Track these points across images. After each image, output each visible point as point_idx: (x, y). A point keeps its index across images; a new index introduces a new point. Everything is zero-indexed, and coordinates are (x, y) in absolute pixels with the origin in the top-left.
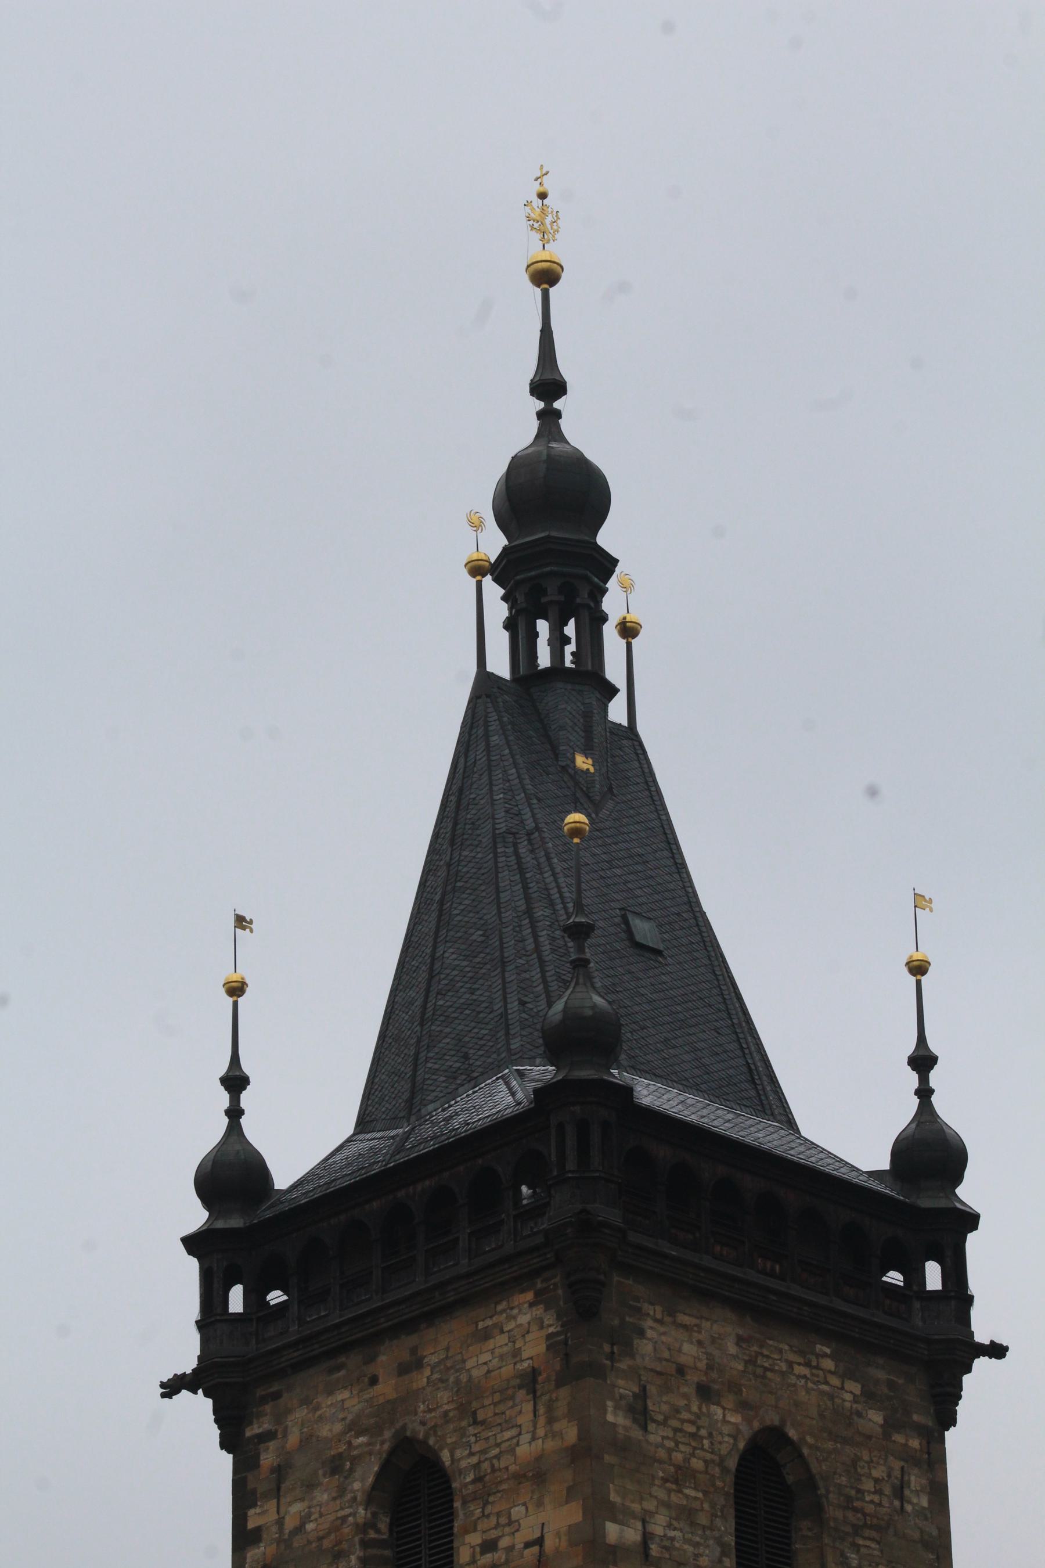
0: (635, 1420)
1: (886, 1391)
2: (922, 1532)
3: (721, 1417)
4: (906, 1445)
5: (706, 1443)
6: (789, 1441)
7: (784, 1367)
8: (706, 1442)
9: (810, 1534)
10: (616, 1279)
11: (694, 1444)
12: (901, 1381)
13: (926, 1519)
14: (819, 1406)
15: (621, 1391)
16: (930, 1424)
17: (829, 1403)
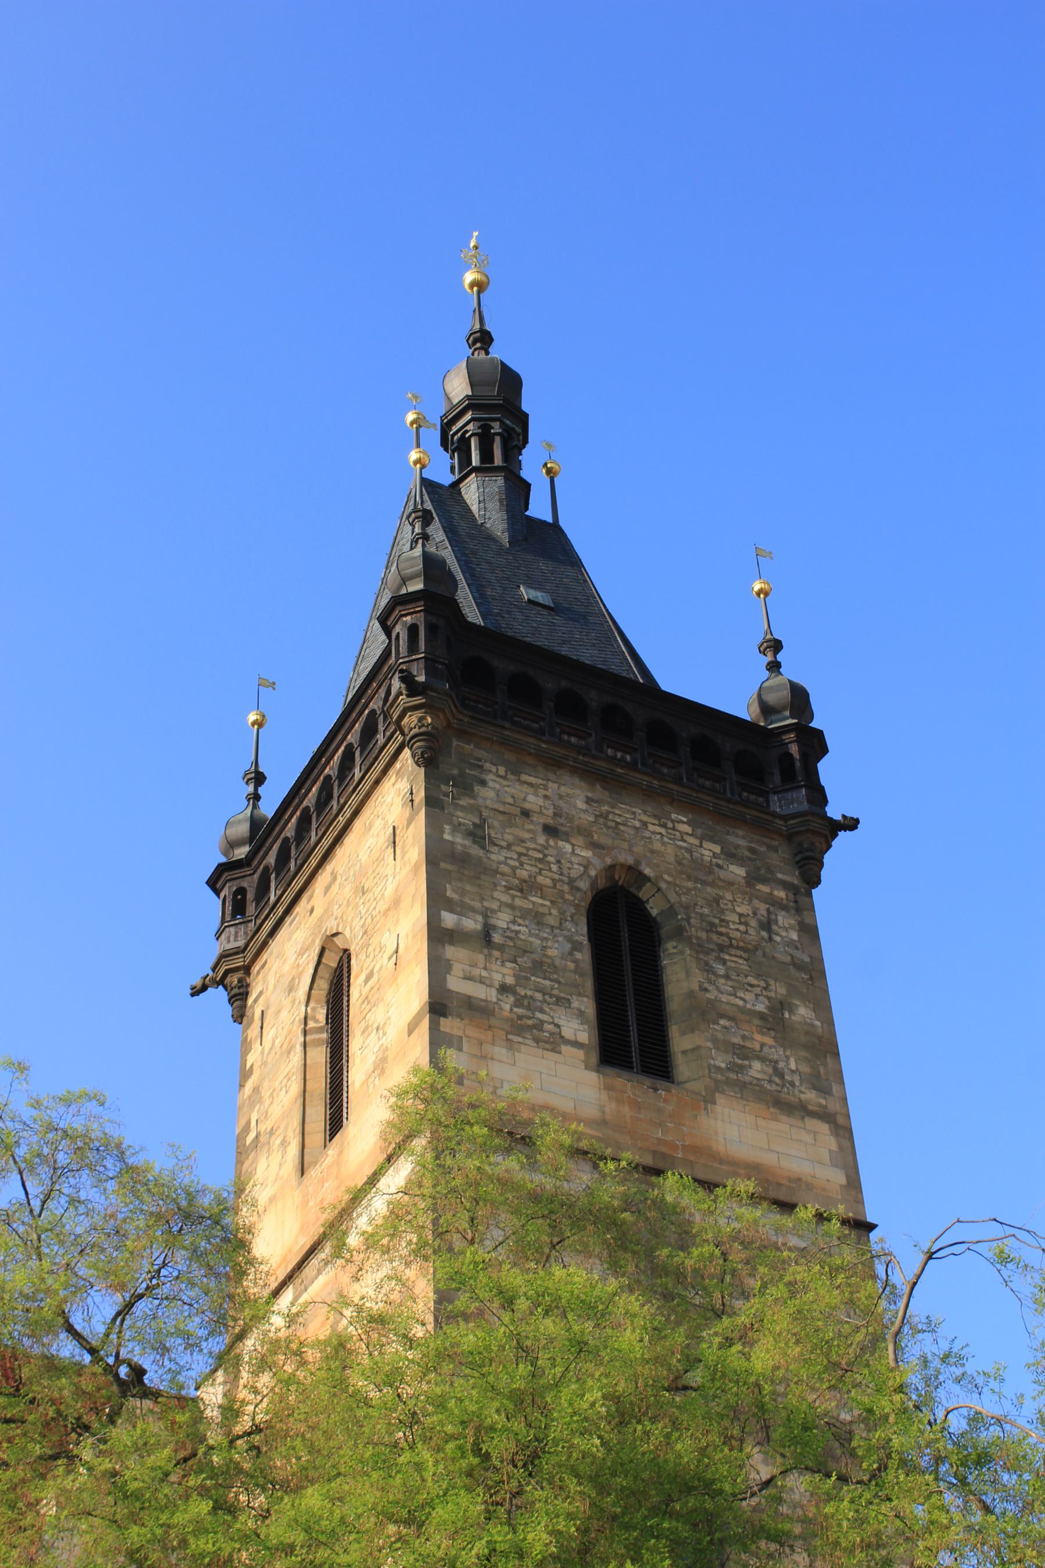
0: (474, 842)
1: (747, 853)
2: (792, 957)
3: (570, 850)
4: (771, 894)
5: (554, 868)
6: (647, 879)
7: (637, 824)
8: (554, 868)
9: (675, 951)
10: (455, 743)
11: (540, 866)
12: (763, 849)
13: (797, 948)
14: (676, 855)
15: (460, 819)
16: (796, 882)
17: (687, 855)
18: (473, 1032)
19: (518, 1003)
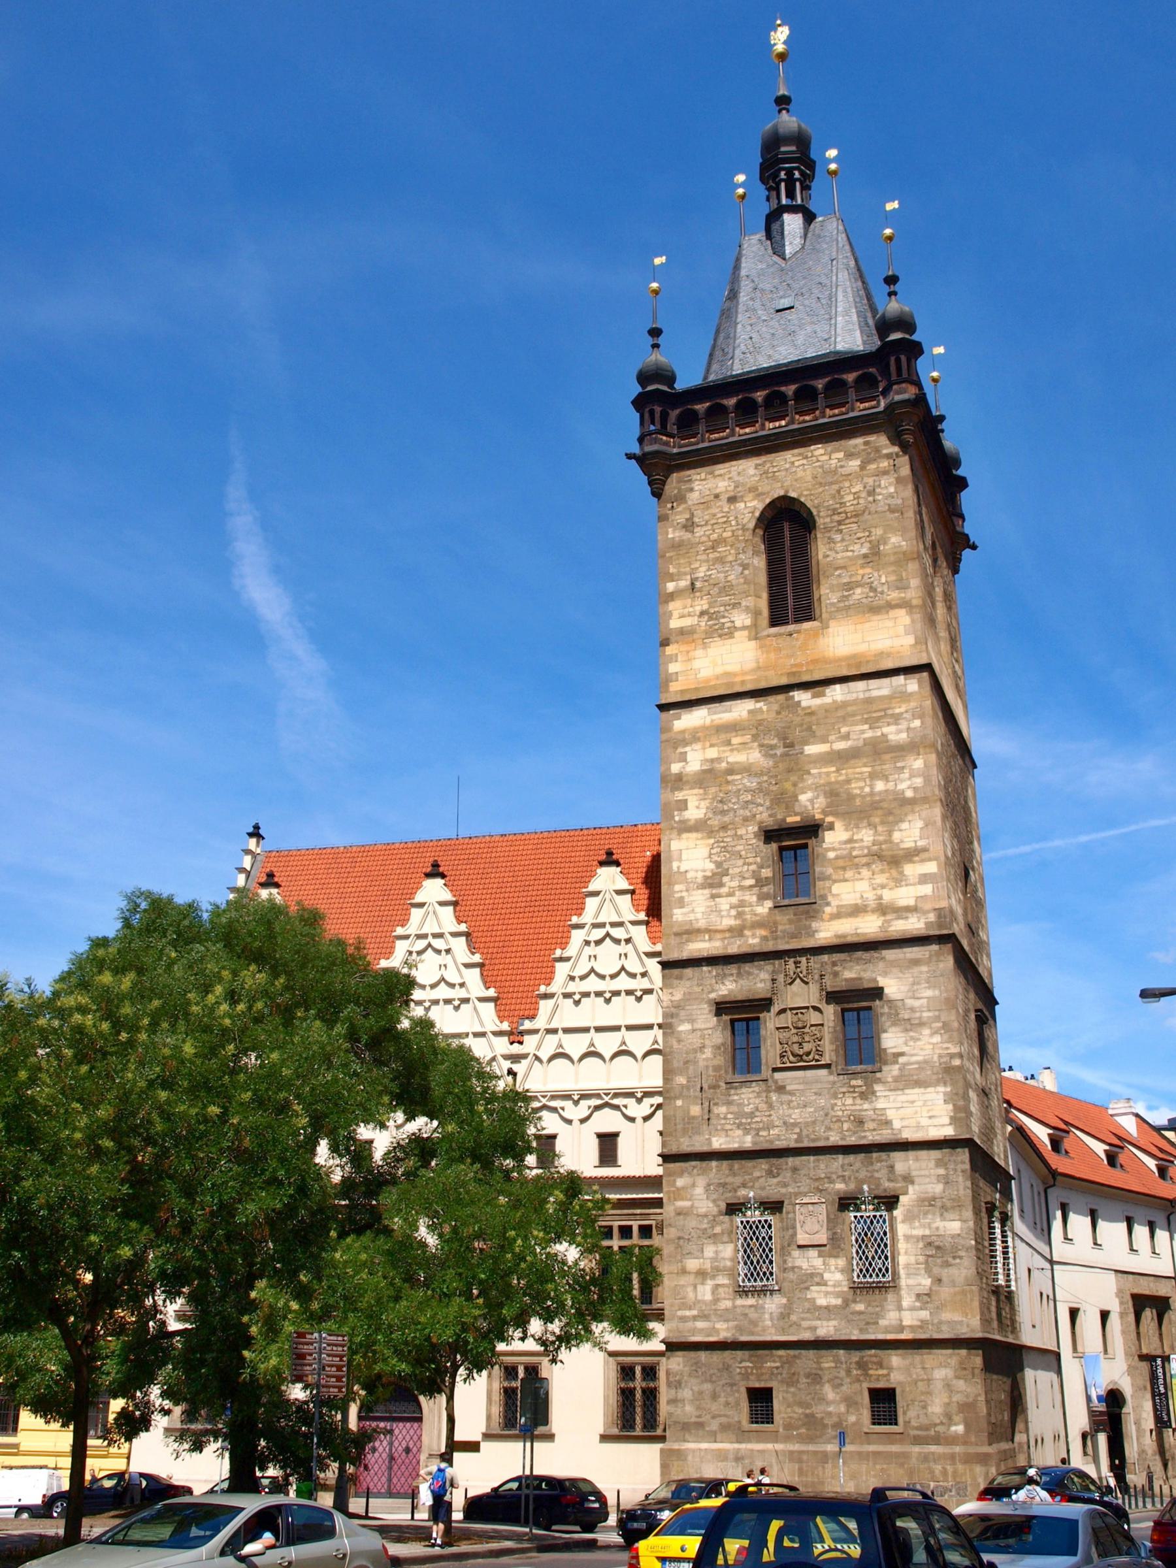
5: (733, 523)
7: (787, 466)
8: (733, 523)
18: (684, 648)
19: (710, 619)
